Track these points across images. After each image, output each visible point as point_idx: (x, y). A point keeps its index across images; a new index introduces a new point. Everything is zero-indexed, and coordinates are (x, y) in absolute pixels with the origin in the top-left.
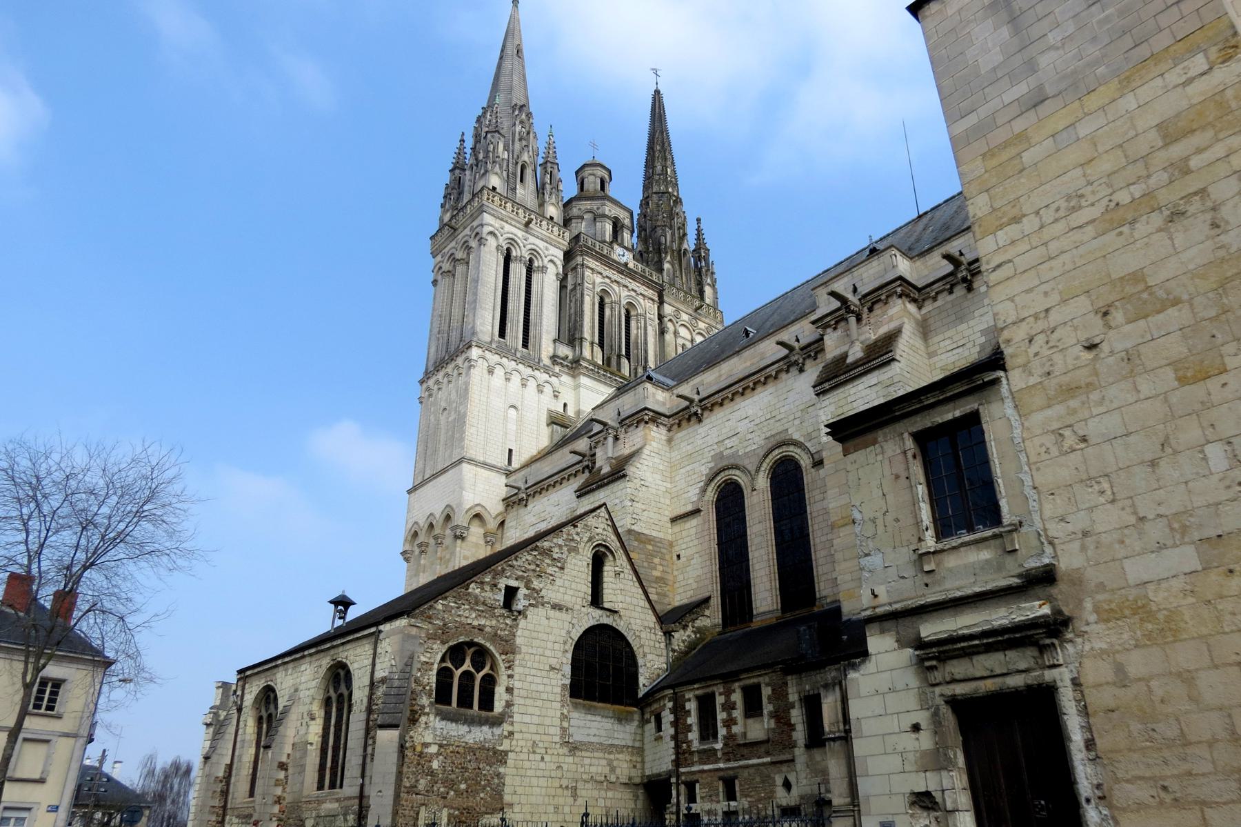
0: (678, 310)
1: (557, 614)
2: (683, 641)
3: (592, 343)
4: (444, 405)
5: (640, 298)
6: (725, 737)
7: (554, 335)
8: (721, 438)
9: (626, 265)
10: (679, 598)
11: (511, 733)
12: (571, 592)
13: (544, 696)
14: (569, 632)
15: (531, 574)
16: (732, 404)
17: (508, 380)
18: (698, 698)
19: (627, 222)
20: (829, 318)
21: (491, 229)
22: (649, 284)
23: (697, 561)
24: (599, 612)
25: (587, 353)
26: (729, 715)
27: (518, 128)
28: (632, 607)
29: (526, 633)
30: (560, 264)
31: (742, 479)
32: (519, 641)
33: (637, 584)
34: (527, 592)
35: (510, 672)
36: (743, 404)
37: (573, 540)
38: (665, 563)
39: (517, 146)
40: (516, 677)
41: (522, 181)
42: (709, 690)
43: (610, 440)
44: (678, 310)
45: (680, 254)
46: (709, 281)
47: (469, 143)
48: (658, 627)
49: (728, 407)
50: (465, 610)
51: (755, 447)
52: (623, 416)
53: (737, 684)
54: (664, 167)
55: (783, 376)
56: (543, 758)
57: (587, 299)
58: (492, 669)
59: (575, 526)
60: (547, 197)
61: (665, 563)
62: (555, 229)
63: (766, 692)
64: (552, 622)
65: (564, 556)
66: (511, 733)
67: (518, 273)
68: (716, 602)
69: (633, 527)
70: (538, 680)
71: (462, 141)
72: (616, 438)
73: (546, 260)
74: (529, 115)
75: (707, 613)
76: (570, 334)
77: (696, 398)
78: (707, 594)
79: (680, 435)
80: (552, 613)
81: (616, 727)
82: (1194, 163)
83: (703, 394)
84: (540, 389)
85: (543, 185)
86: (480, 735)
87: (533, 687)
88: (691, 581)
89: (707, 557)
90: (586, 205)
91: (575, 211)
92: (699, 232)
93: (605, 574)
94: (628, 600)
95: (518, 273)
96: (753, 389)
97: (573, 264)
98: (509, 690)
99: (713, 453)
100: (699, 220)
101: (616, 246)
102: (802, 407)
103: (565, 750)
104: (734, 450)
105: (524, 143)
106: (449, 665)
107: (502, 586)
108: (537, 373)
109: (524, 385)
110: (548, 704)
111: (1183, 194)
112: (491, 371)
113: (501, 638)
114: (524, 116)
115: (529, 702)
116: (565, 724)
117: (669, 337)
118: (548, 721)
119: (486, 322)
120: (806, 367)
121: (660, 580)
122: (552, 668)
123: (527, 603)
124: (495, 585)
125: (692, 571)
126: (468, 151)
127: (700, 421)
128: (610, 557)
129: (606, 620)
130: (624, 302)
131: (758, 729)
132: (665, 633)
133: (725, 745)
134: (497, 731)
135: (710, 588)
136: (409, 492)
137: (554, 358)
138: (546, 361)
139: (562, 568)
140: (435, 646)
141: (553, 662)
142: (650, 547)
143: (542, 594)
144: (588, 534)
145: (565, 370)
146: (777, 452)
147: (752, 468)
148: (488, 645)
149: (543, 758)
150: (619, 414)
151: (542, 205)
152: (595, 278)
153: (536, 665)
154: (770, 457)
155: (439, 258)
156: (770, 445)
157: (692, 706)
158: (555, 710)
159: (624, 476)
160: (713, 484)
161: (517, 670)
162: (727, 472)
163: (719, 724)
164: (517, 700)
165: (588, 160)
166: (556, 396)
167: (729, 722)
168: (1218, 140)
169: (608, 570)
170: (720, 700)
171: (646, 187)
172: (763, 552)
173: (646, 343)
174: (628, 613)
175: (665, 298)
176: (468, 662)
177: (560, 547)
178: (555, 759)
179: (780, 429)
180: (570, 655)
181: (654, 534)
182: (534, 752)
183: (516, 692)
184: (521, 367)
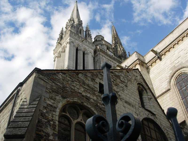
41: (80, 33)
71: (63, 29)
78: (183, 120)
80: (126, 105)
94: (157, 111)
104: (179, 63)
128: (145, 91)
135: (184, 117)
140: (57, 98)
160: (173, 78)
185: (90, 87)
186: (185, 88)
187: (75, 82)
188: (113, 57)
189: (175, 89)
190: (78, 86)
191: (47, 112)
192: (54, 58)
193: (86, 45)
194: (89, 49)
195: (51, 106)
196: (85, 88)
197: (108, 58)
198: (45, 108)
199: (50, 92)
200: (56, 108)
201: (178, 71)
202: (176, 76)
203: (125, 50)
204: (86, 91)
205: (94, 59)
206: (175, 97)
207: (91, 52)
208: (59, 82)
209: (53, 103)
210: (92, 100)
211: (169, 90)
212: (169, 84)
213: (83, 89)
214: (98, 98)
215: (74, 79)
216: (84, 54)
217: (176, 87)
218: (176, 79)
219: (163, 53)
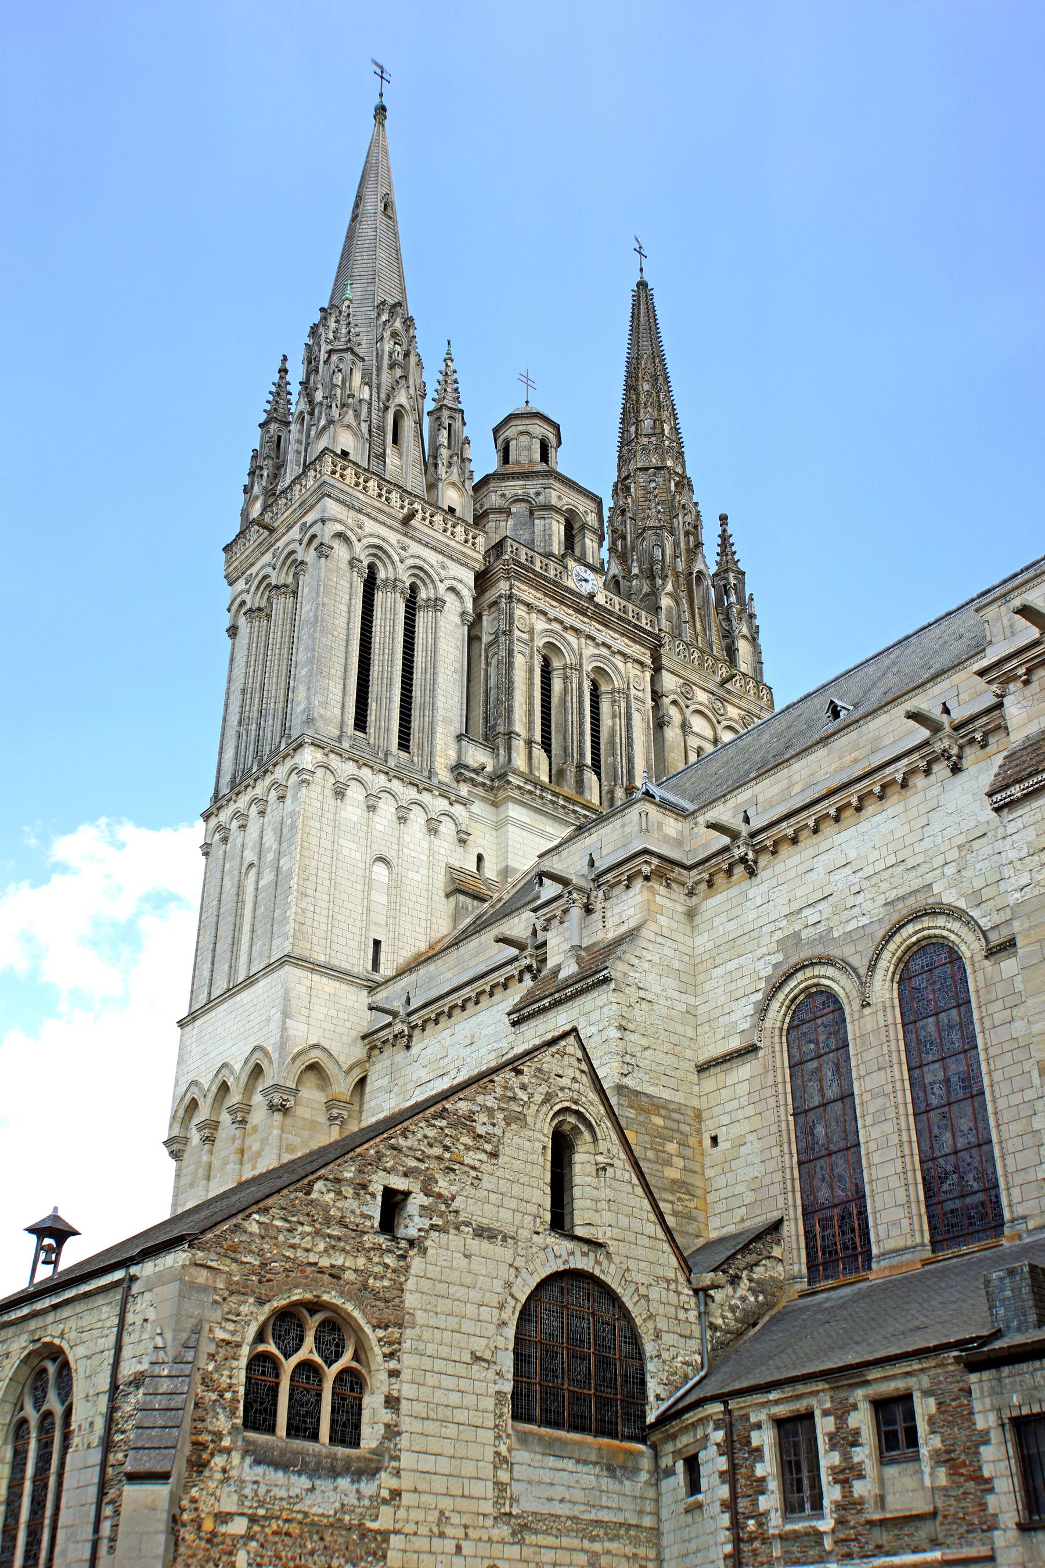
1: (485, 1245)
2: (733, 1309)
3: (529, 743)
4: (250, 856)
5: (618, 661)
6: (839, 1506)
7: (457, 725)
8: (794, 907)
9: (591, 596)
10: (722, 1222)
11: (396, 1494)
12: (513, 1204)
13: (461, 1416)
14: (509, 1285)
15: (433, 1164)
16: (815, 839)
17: (372, 808)
18: (780, 1423)
19: (591, 519)
20: (1015, 662)
21: (339, 528)
22: (635, 633)
23: (752, 1147)
24: (569, 1245)
25: (519, 761)
26: (846, 1457)
27: (388, 346)
28: (630, 1237)
29: (425, 1285)
30: (468, 594)
31: (841, 985)
32: (411, 1300)
33: (639, 1190)
34: (427, 1201)
35: (393, 1365)
36: (838, 839)
37: (514, 1098)
38: (688, 1152)
39: (386, 378)
40: (405, 1376)
41: (395, 441)
42: (801, 1406)
43: (576, 912)
44: (688, 683)
45: (692, 580)
46: (745, 631)
47: (297, 373)
48: (682, 1279)
49: (809, 845)
50: (304, 1235)
51: (865, 921)
52: (601, 865)
53: (860, 1393)
54: (658, 422)
55: (919, 781)
56: (459, 1548)
57: (519, 661)
58: (356, 1357)
59: (518, 1072)
60: (442, 470)
61: (688, 1152)
62: (459, 529)
63: (924, 1408)
64: (477, 1265)
65: (498, 1131)
66: (396, 1494)
67: (390, 608)
68: (794, 1230)
69: (627, 1081)
70: (449, 1382)
71: (283, 371)
72: (588, 910)
73: (442, 588)
74: (409, 322)
75: (777, 1252)
77: (744, 830)
78: (776, 1215)
79: (712, 902)
80: (476, 1245)
81: (606, 1483)
83: (756, 824)
84: (432, 828)
85: (435, 448)
86: (327, 1499)
87: (440, 1396)
88: (740, 1189)
89: (772, 1140)
90: (515, 488)
91: (494, 500)
92: (725, 540)
93: (577, 1168)
94: (624, 1221)
95: (390, 608)
96: (858, 809)
97: (491, 595)
98: (392, 1402)
99: (778, 935)
100: (723, 519)
101: (571, 563)
102: (961, 840)
103: (504, 1531)
104: (821, 928)
105: (399, 372)
106: (271, 1347)
107: (377, 1188)
108: (426, 798)
109: (402, 820)
110: (468, 1434)
112: (339, 793)
113: (376, 1294)
114: (398, 324)
115: (431, 1427)
116: (504, 1476)
117: (672, 734)
118: (468, 1469)
119: (331, 700)
120: (965, 763)
121: (677, 1186)
122: (477, 1359)
123: (426, 1223)
124: (364, 1187)
125: (746, 1166)
126: (295, 388)
128: (587, 1136)
129: (582, 1262)
130: (588, 667)
131: (911, 1487)
132: (696, 1291)
133: (840, 1522)
134: (368, 1488)
135: (781, 1203)
136: (182, 1024)
137: (459, 769)
138: (444, 775)
139: (494, 1155)
140: (244, 1309)
141: (479, 1345)
142: (659, 1121)
143: (455, 1205)
144: (543, 1089)
145: (480, 791)
146: (910, 929)
147: (861, 963)
148: (349, 1307)
149: (459, 1548)
150: (592, 863)
151: (432, 487)
152: (534, 622)
153: (444, 1352)
154: (897, 939)
155: (241, 585)
156: (895, 917)
157: (765, 1438)
158: (484, 1445)
159: (606, 980)
160: (781, 996)
161: (408, 1361)
162: (809, 972)
163: (825, 1478)
164: (407, 1424)
165: (519, 406)
166: (462, 841)
167: (847, 1474)
169: (582, 1159)
170: (824, 1425)
171: (623, 461)
172: (888, 1127)
173: (630, 744)
174: (623, 1248)
175: (665, 661)
176: (309, 1340)
177: (490, 1111)
178: (484, 1549)
179: (916, 884)
180: (510, 1332)
181: (666, 1094)
182: (442, 1535)
183: (405, 1405)
184: (396, 785)
185: (346, 1227)
186: (814, 1064)
187: (300, 1228)
188: (597, 605)
189: (778, 1054)
190: (307, 1242)
191: (217, 1369)
192: (229, 610)
193: (426, 545)
194: (444, 567)
195: (228, 1343)
196: (330, 1236)
197: (562, 617)
198: (212, 1357)
199: (224, 1299)
200: (239, 1345)
201: (804, 967)
202: (792, 990)
203: (696, 504)
204: (333, 1247)
205: (474, 626)
206: (769, 1092)
207: (459, 587)
208: (251, 1252)
209: (233, 1333)
210: (349, 1276)
211: (752, 1049)
212: (756, 1018)
213: (322, 1246)
214: (370, 1259)
215: (295, 1219)
217: (785, 1046)
218: (793, 1007)
219: (767, 839)
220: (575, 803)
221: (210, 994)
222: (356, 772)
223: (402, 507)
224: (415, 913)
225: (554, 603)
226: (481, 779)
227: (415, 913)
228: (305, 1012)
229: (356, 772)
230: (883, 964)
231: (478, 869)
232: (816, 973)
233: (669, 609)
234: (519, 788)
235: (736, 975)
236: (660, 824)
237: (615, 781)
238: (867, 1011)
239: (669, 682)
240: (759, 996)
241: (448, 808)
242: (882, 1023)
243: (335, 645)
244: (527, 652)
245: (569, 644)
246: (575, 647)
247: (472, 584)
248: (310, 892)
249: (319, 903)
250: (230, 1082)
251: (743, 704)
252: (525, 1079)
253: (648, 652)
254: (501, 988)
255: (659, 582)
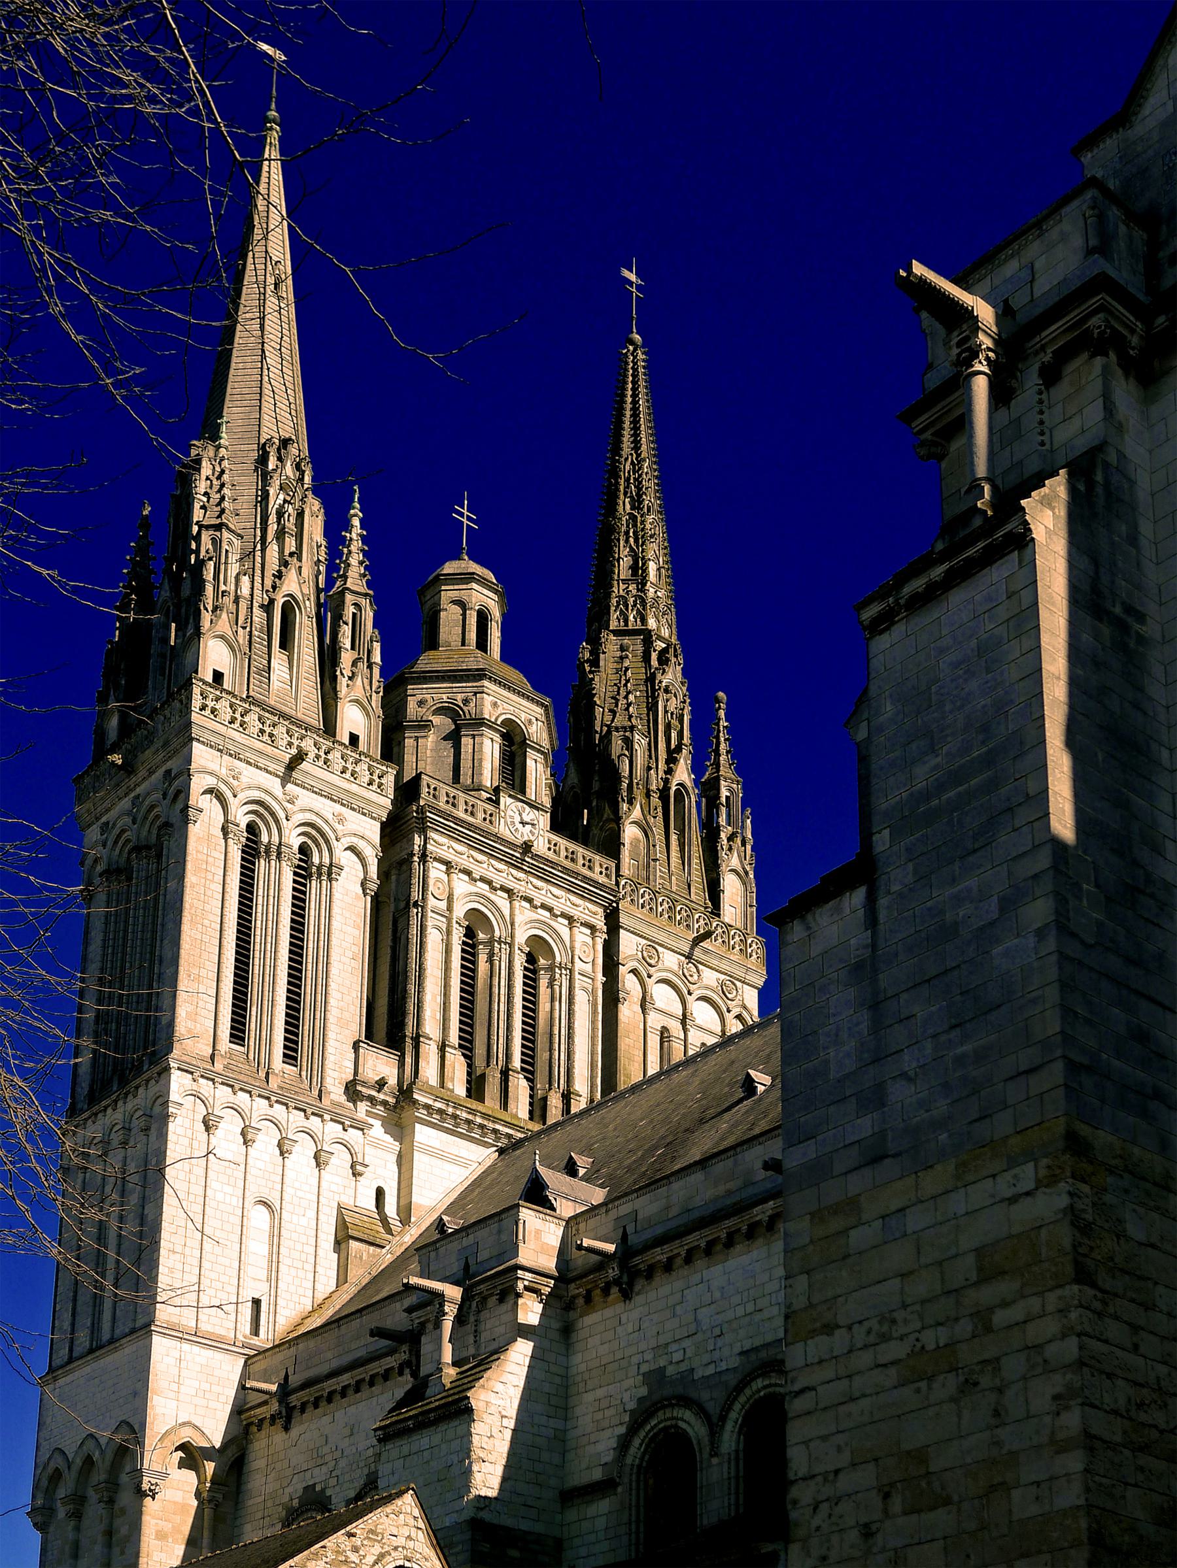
0: (653, 944)
3: (442, 1048)
8: (662, 1340)
9: (527, 847)
25: (429, 1071)
30: (372, 855)
62: (362, 768)
67: (278, 880)
73: (338, 847)
76: (390, 1022)
79: (589, 1320)
82: (1000, 1318)
95: (278, 880)
104: (683, 1367)
111: (981, 1358)
117: (628, 1012)
127: (627, 1295)
138: (336, 1093)
142: (514, 1553)
152: (453, 883)
168: (1023, 1297)
181: (524, 1526)
197: (490, 874)
207: (361, 845)
216: (304, 873)
220: (496, 1120)
221: (71, 1350)
222: (232, 1098)
223: (290, 744)
224: (300, 1265)
225: (480, 857)
226: (381, 1096)
227: (300, 1265)
228: (174, 1387)
229: (232, 1098)
230: (733, 1415)
231: (377, 1208)
232: (675, 1414)
233: (635, 842)
234: (427, 1107)
235: (604, 1404)
236: (538, 1232)
237: (550, 1084)
238: (715, 1461)
239: (628, 944)
240: (622, 1430)
241: (342, 1134)
242: (725, 1476)
243: (206, 938)
244: (444, 927)
245: (498, 910)
246: (506, 913)
247: (377, 839)
248: (178, 1249)
249: (189, 1260)
250: (96, 1456)
251: (724, 966)
252: (357, 1541)
253: (600, 911)
254: (380, 1380)
255: (625, 806)
